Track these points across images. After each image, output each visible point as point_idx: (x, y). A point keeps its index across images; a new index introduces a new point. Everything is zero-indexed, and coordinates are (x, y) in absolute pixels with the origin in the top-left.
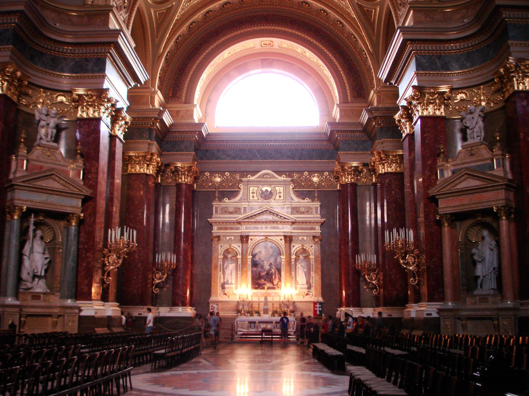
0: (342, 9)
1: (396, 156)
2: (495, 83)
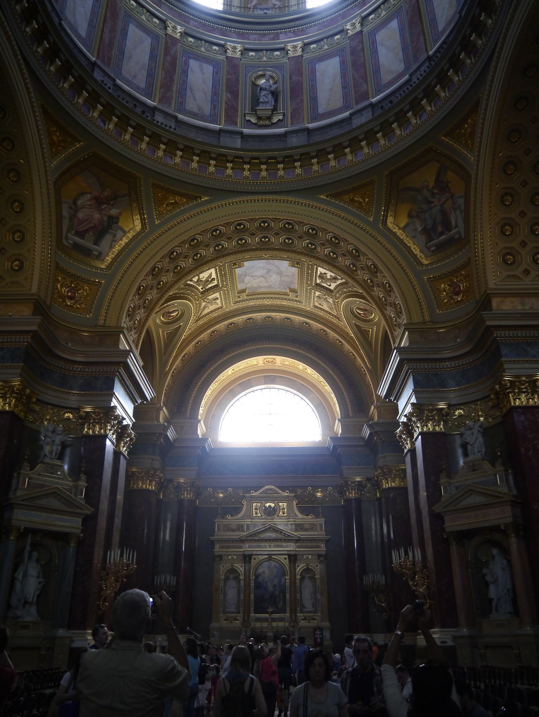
0: (341, 329)
2: (492, 399)
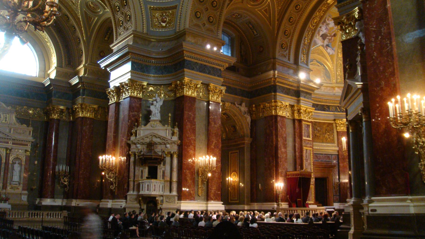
0: (73, 10)
1: (91, 108)
